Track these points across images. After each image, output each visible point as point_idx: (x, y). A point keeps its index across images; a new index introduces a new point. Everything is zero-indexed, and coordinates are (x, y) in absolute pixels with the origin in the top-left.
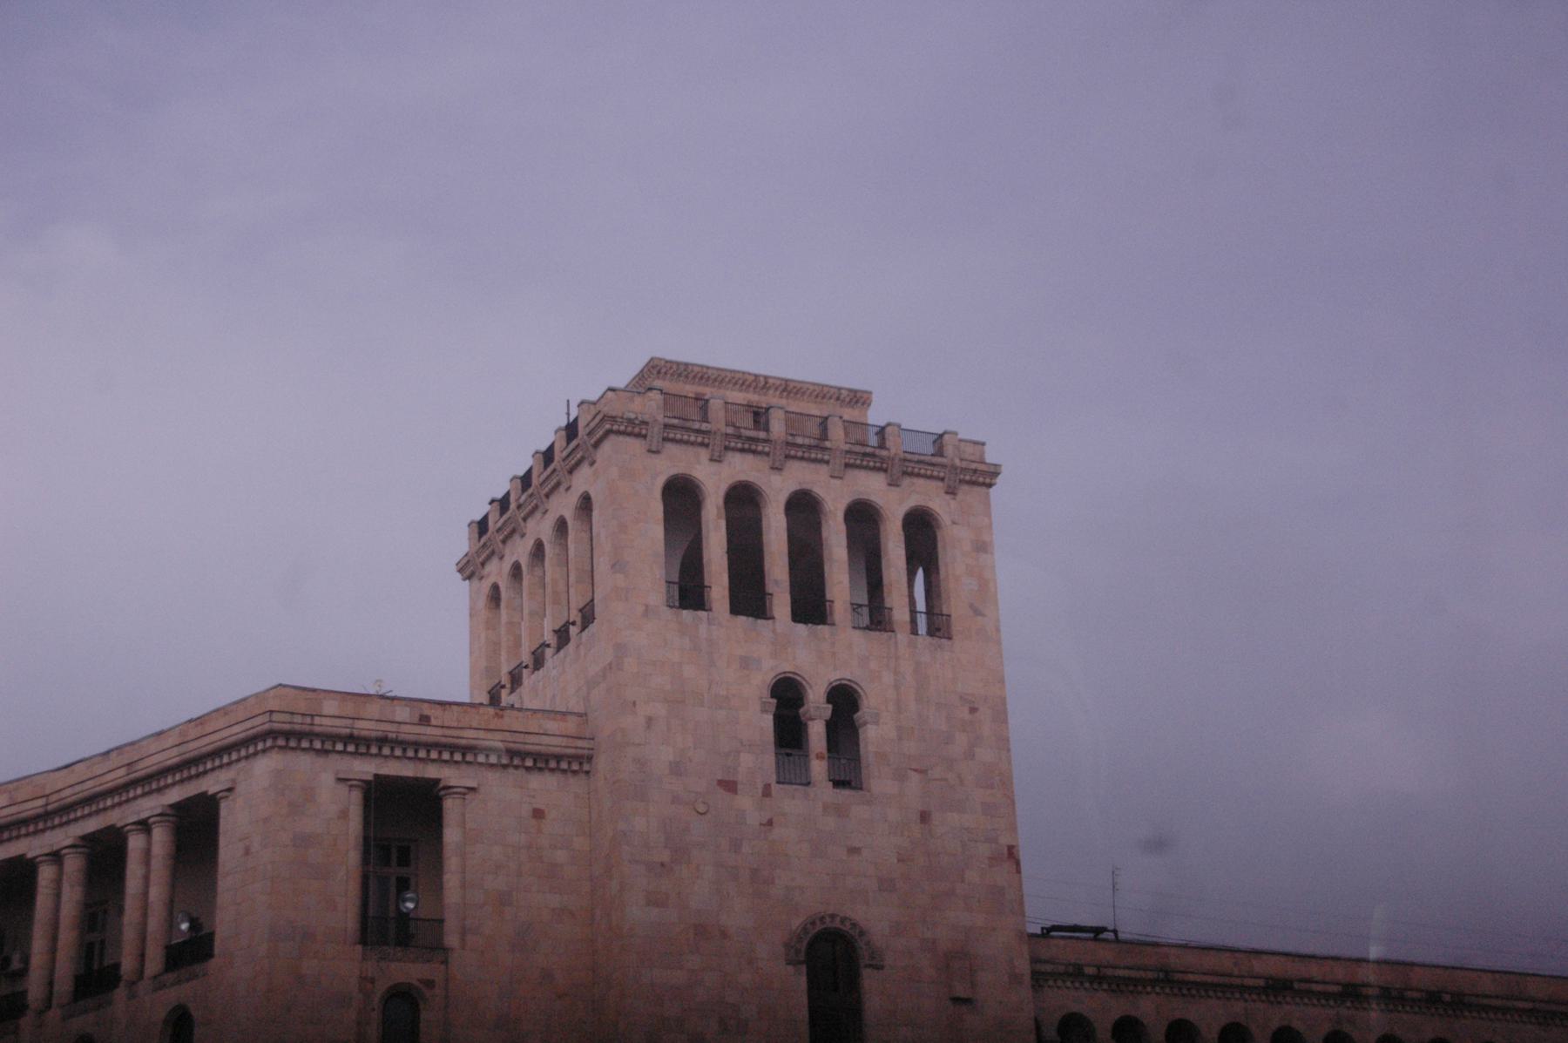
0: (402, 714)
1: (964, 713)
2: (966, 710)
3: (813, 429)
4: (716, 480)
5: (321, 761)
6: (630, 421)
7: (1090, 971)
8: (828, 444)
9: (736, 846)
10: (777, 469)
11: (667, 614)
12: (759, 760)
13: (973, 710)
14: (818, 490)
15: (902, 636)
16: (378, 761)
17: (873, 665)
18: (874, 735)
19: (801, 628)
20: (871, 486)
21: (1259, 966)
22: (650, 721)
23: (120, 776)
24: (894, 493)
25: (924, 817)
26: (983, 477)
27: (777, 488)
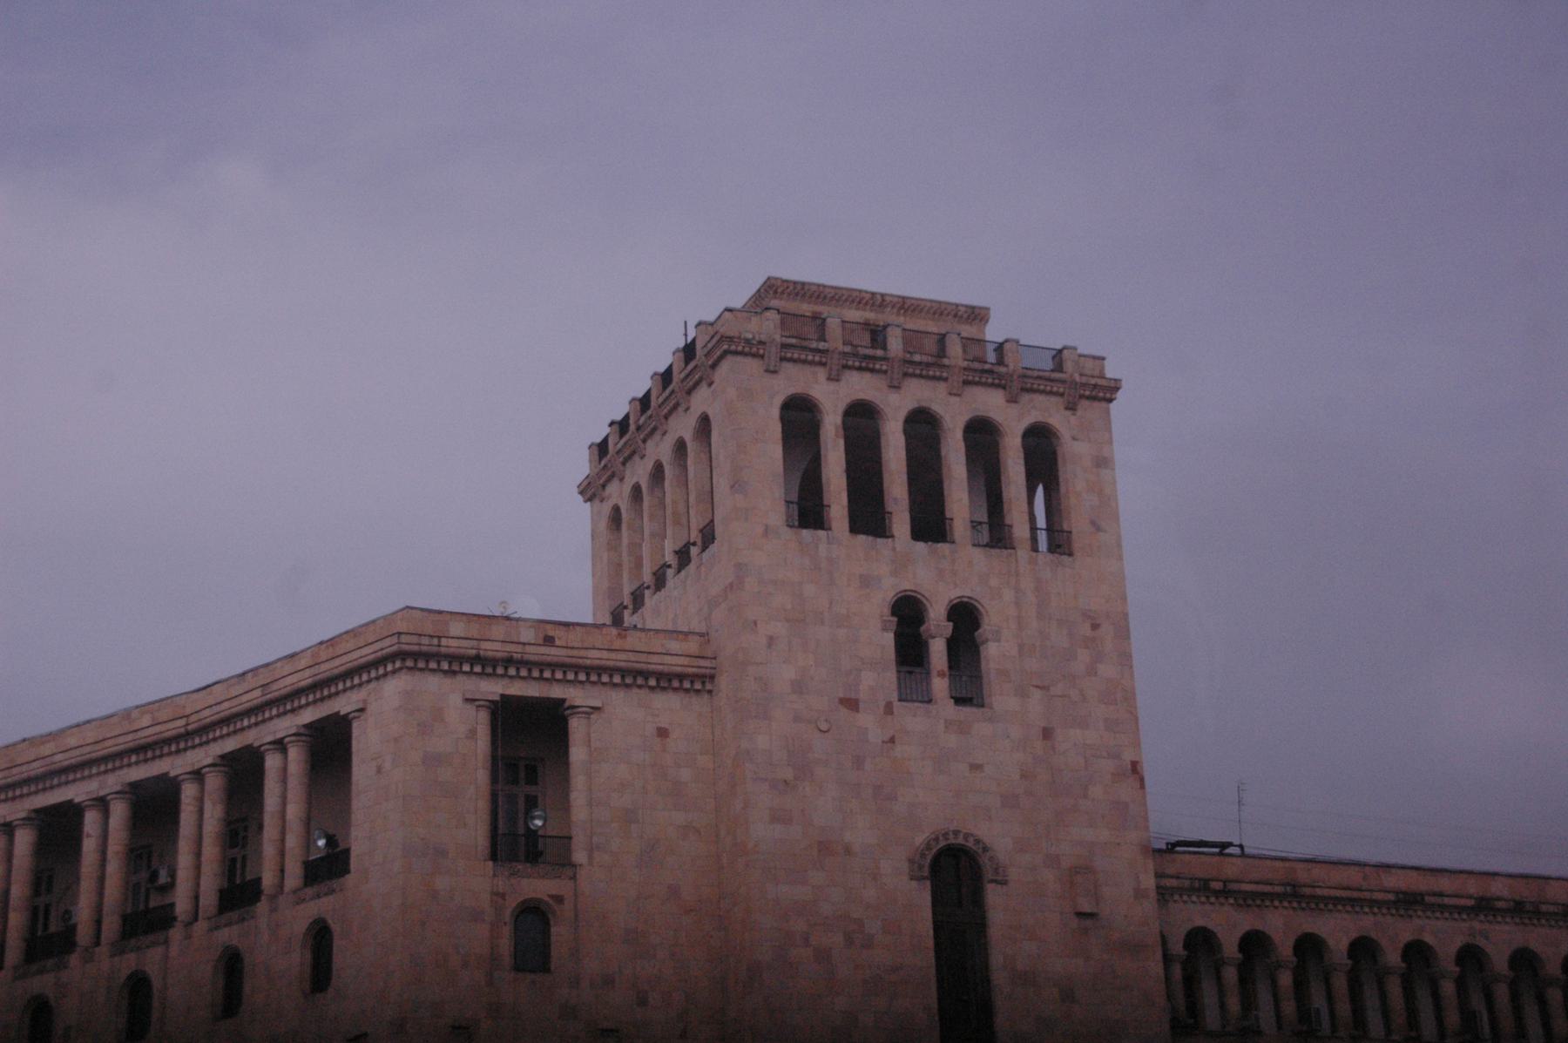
0: (527, 635)
1: (1085, 629)
2: (1087, 626)
3: (930, 345)
4: (833, 399)
5: (447, 682)
6: (747, 341)
7: (1217, 885)
8: (946, 361)
9: (859, 762)
10: (895, 387)
11: (787, 533)
12: (880, 679)
13: (1095, 627)
14: (937, 408)
15: (1023, 553)
16: (506, 681)
17: (994, 582)
18: (995, 653)
19: (921, 546)
20: (990, 403)
21: (1392, 881)
22: (771, 640)
23: (256, 697)
24: (1013, 410)
25: (1047, 733)
26: (1104, 392)
27: (895, 408)
